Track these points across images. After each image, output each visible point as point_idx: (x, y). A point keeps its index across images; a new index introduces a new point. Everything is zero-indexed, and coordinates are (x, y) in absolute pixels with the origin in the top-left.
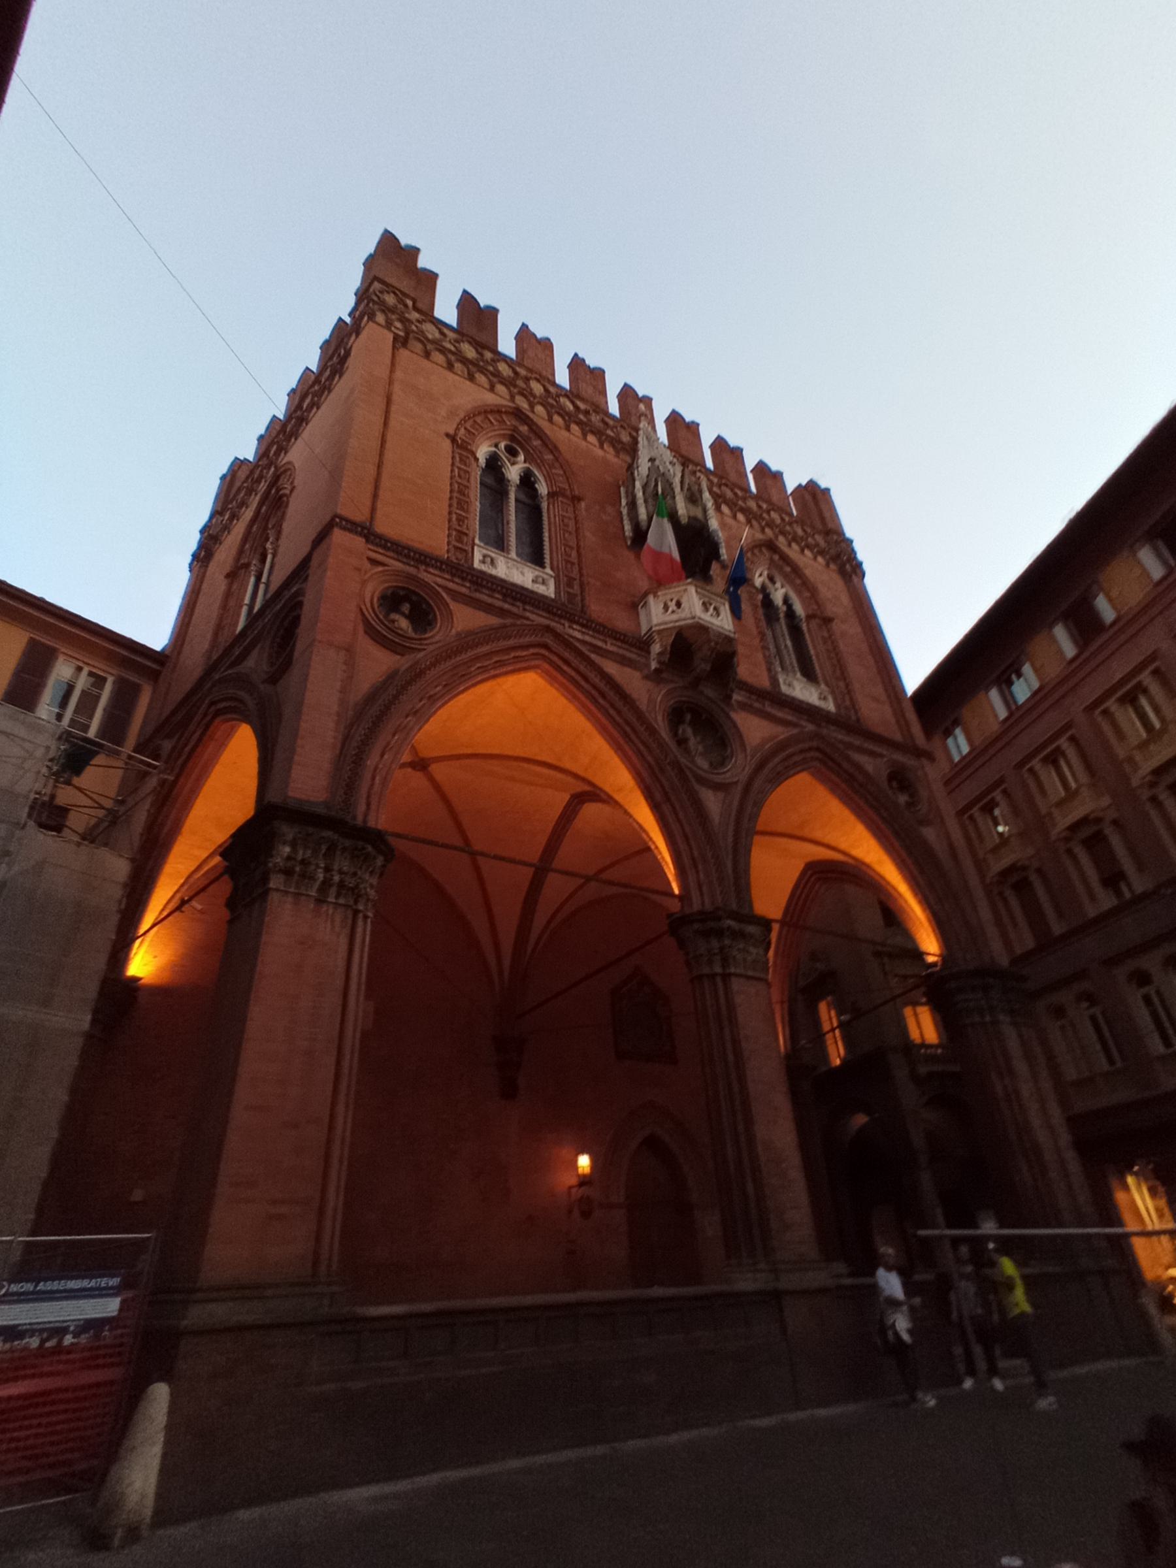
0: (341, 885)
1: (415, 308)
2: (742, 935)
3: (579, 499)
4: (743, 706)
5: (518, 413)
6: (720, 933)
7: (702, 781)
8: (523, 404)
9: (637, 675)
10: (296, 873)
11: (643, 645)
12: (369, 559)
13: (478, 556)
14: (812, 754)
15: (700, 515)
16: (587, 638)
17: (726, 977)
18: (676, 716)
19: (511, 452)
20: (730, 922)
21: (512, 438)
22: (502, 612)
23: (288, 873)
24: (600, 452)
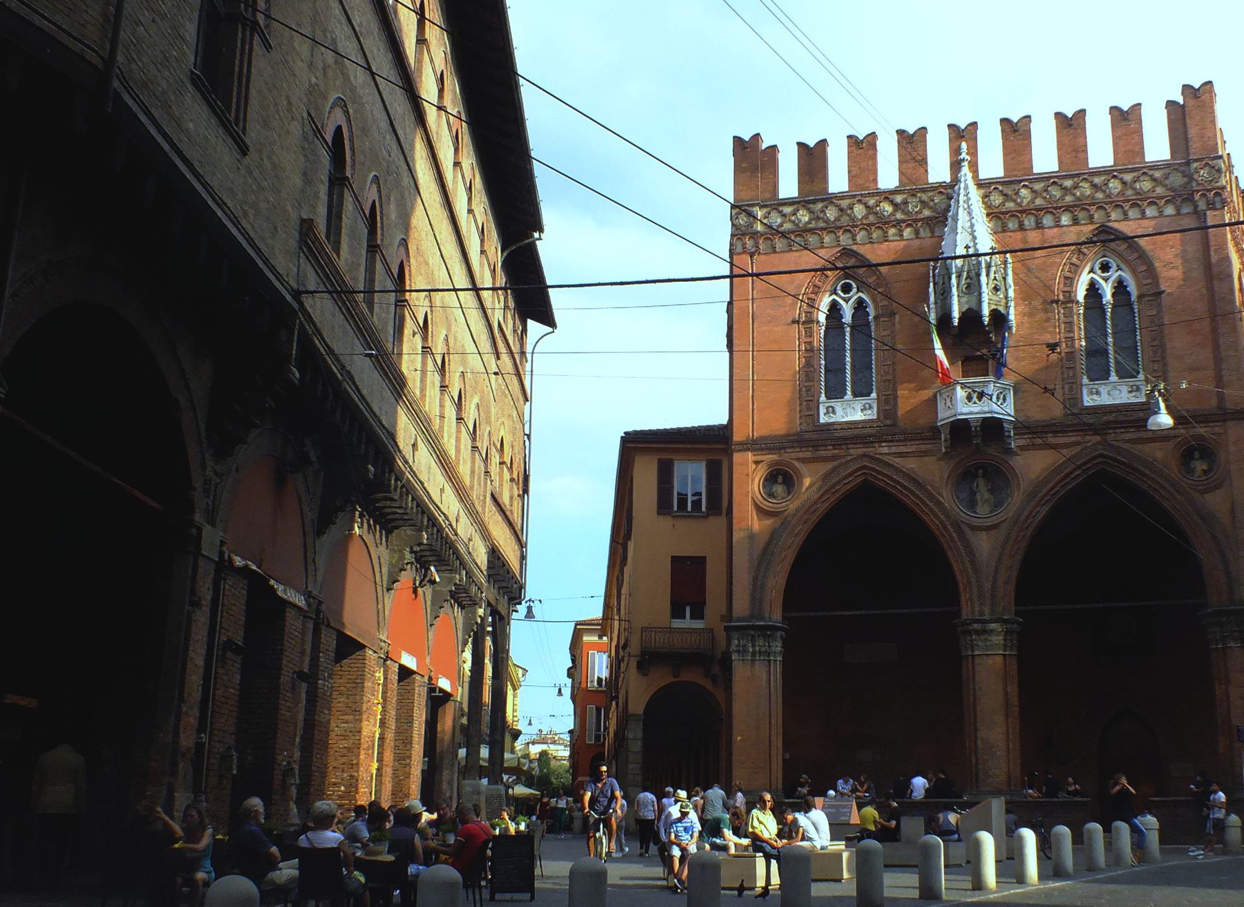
0: (760, 652)
1: (762, 207)
2: (985, 632)
5: (847, 252)
6: (969, 633)
7: (974, 528)
8: (845, 239)
10: (742, 651)
13: (822, 410)
14: (1100, 460)
15: (974, 305)
16: (894, 450)
17: (973, 656)
18: (965, 477)
19: (847, 288)
20: (976, 626)
22: (833, 458)
23: (738, 651)
24: (917, 243)
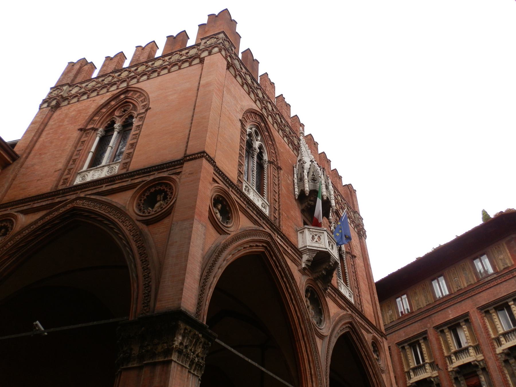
3: (281, 169)
4: (330, 295)
5: (261, 116)
9: (296, 267)
11: (299, 253)
12: (213, 178)
21: (257, 127)
23: (180, 352)
